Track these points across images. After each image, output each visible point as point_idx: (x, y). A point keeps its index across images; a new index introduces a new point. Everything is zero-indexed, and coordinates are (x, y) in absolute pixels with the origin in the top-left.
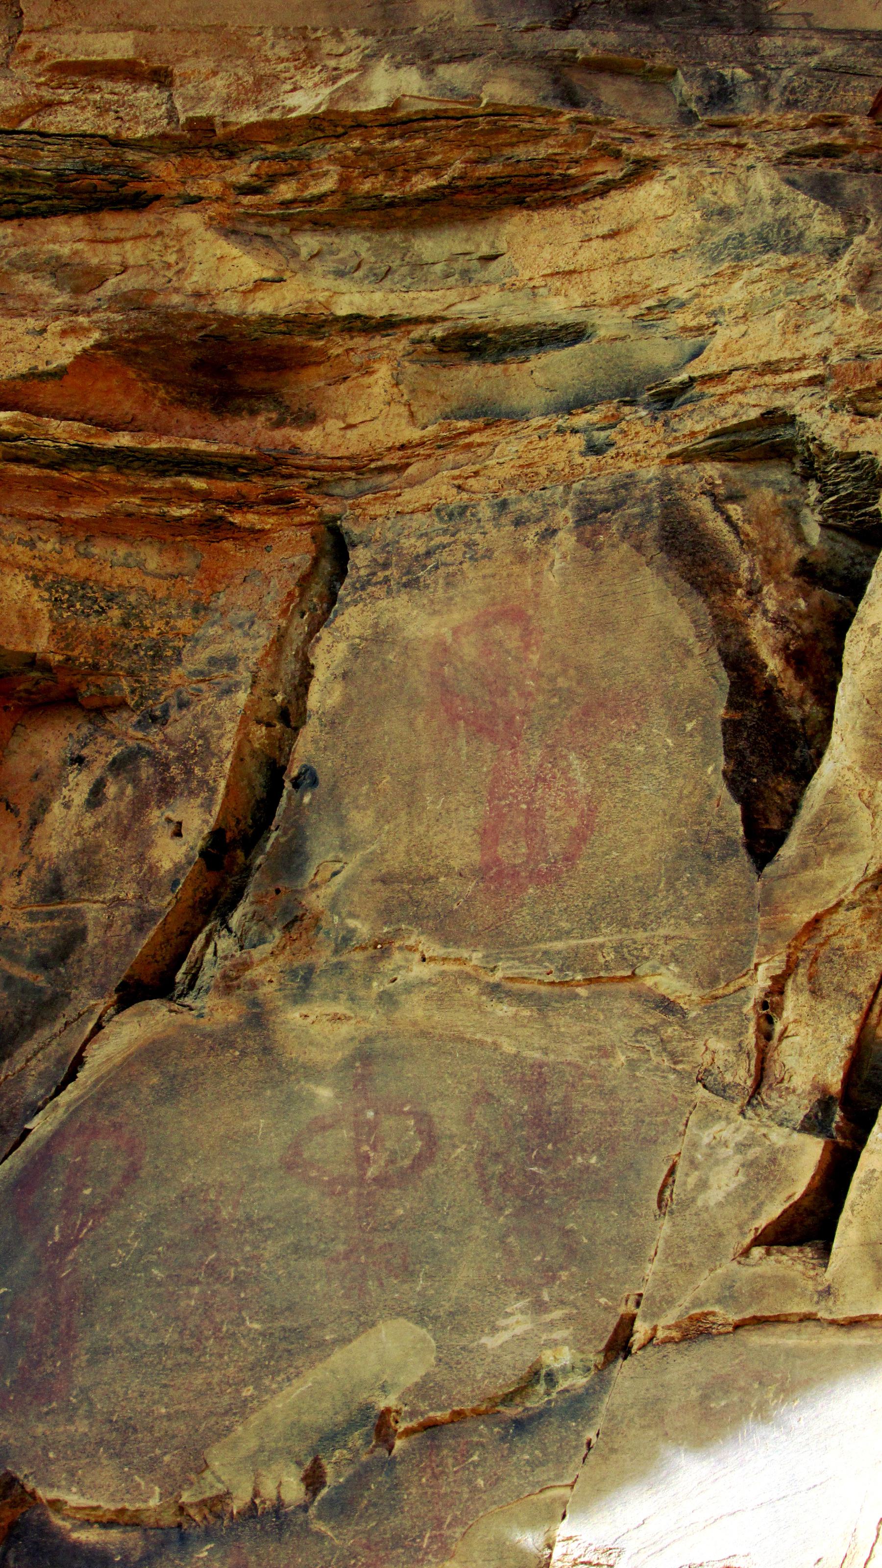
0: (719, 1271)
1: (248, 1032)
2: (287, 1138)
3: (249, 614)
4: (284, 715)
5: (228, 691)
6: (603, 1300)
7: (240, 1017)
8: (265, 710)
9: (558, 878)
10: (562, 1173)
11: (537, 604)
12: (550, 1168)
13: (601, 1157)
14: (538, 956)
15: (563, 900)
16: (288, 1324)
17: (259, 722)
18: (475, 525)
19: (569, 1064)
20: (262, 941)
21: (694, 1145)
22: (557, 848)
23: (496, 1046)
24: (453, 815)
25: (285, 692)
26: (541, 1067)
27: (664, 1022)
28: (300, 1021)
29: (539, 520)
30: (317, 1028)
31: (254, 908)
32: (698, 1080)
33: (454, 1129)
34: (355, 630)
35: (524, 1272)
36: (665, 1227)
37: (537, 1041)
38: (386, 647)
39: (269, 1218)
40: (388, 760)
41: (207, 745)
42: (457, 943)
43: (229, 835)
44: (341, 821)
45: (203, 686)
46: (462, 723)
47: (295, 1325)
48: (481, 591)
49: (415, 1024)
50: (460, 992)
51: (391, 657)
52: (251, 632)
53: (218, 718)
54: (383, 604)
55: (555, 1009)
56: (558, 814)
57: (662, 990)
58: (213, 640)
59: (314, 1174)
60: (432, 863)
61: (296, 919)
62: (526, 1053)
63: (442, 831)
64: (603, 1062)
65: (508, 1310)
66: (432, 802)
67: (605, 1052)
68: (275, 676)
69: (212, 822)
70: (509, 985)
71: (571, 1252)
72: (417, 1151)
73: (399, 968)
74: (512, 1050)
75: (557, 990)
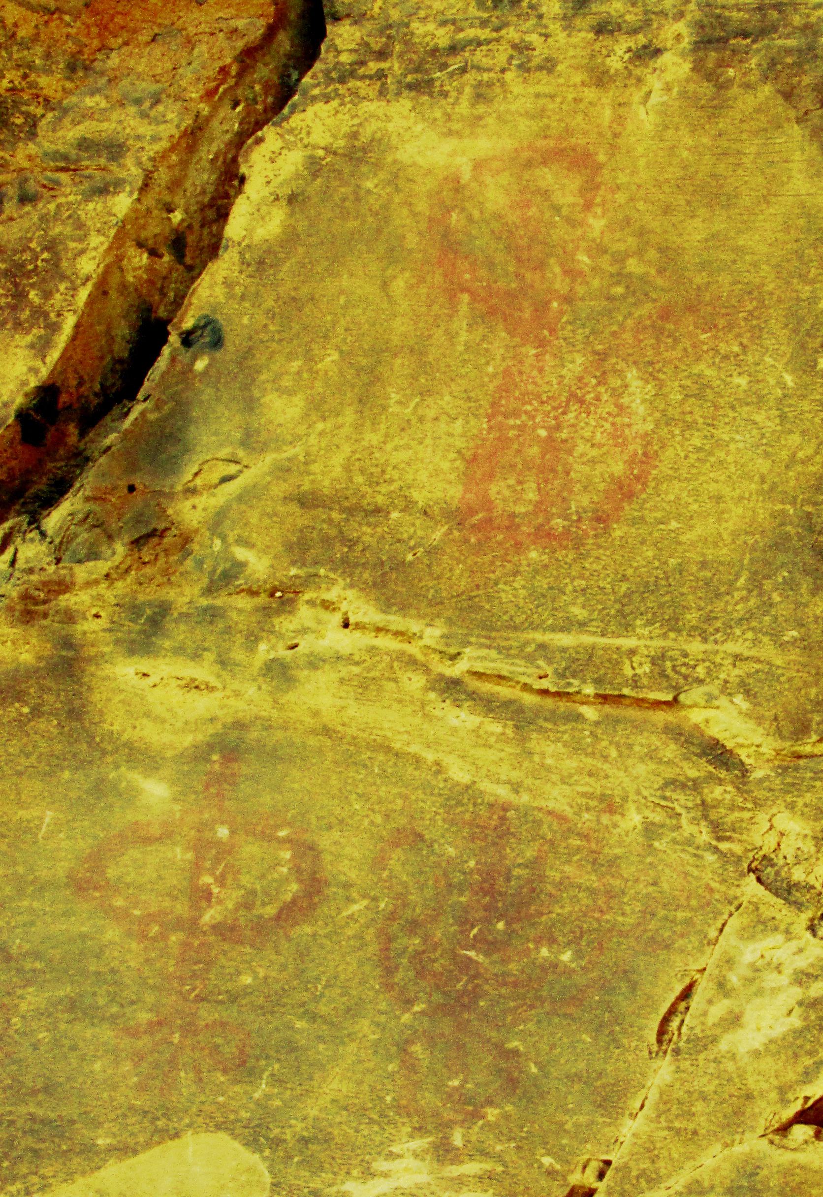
0: (737, 1149)
1: (49, 683)
2: (84, 845)
3: (154, 87)
4: (178, 243)
5: (103, 191)
6: (547, 1161)
7: (39, 658)
8: (153, 229)
9: (578, 544)
10: (513, 967)
11: (613, 149)
12: (495, 957)
13: (579, 955)
14: (530, 649)
15: (582, 576)
16: (40, 1112)
17: (140, 245)
18: (533, 21)
19: (550, 813)
20: (93, 555)
21: (729, 962)
22: (585, 501)
23: (439, 768)
24: (428, 426)
25: (186, 211)
26: (505, 810)
27: (710, 778)
28: (136, 681)
29: (635, 31)
30: (158, 696)
31: (88, 507)
32: (750, 870)
33: (353, 875)
34: (320, 137)
35: (428, 1099)
36: (663, 1071)
37: (505, 772)
38: (364, 169)
39: (37, 955)
40: (340, 330)
41: (55, 262)
42: (404, 608)
43: (64, 398)
44: (250, 405)
45: (64, 177)
46: (466, 297)
47: (53, 1115)
48: (527, 114)
49: (316, 714)
50: (396, 681)
51: (369, 185)
52: (153, 113)
53: (80, 225)
54: (367, 107)
55: (541, 730)
56: (595, 452)
57: (714, 731)
58: (89, 115)
59: (119, 902)
60: (384, 489)
61: (153, 534)
62: (486, 786)
63: (408, 447)
64: (605, 819)
65: (395, 1149)
66: (399, 403)
67: (610, 805)
68: (175, 185)
69: (44, 372)
70: (474, 684)
71: (512, 1083)
72: (288, 897)
73: (304, 631)
74: (464, 778)
75: (549, 702)
